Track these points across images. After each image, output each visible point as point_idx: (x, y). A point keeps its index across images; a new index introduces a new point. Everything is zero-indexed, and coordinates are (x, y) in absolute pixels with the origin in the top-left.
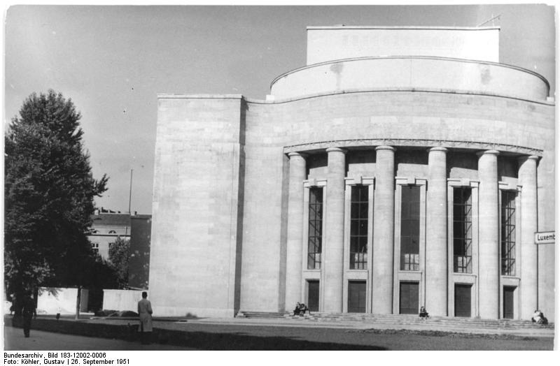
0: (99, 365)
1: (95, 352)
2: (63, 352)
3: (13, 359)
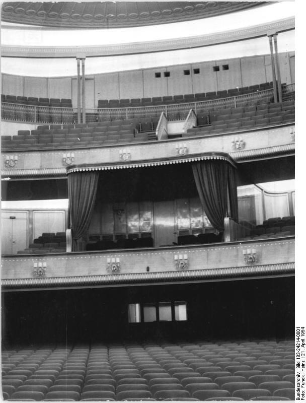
1: (296, 334)
2: (296, 357)
3: (301, 393)
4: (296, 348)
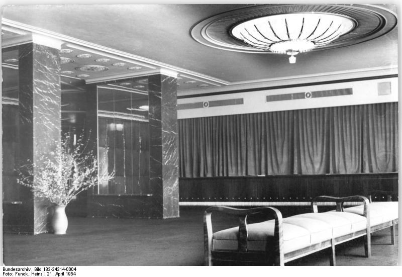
0: (37, 276)
1: (68, 267)
2: (45, 267)
3: (10, 272)
4: (55, 267)
